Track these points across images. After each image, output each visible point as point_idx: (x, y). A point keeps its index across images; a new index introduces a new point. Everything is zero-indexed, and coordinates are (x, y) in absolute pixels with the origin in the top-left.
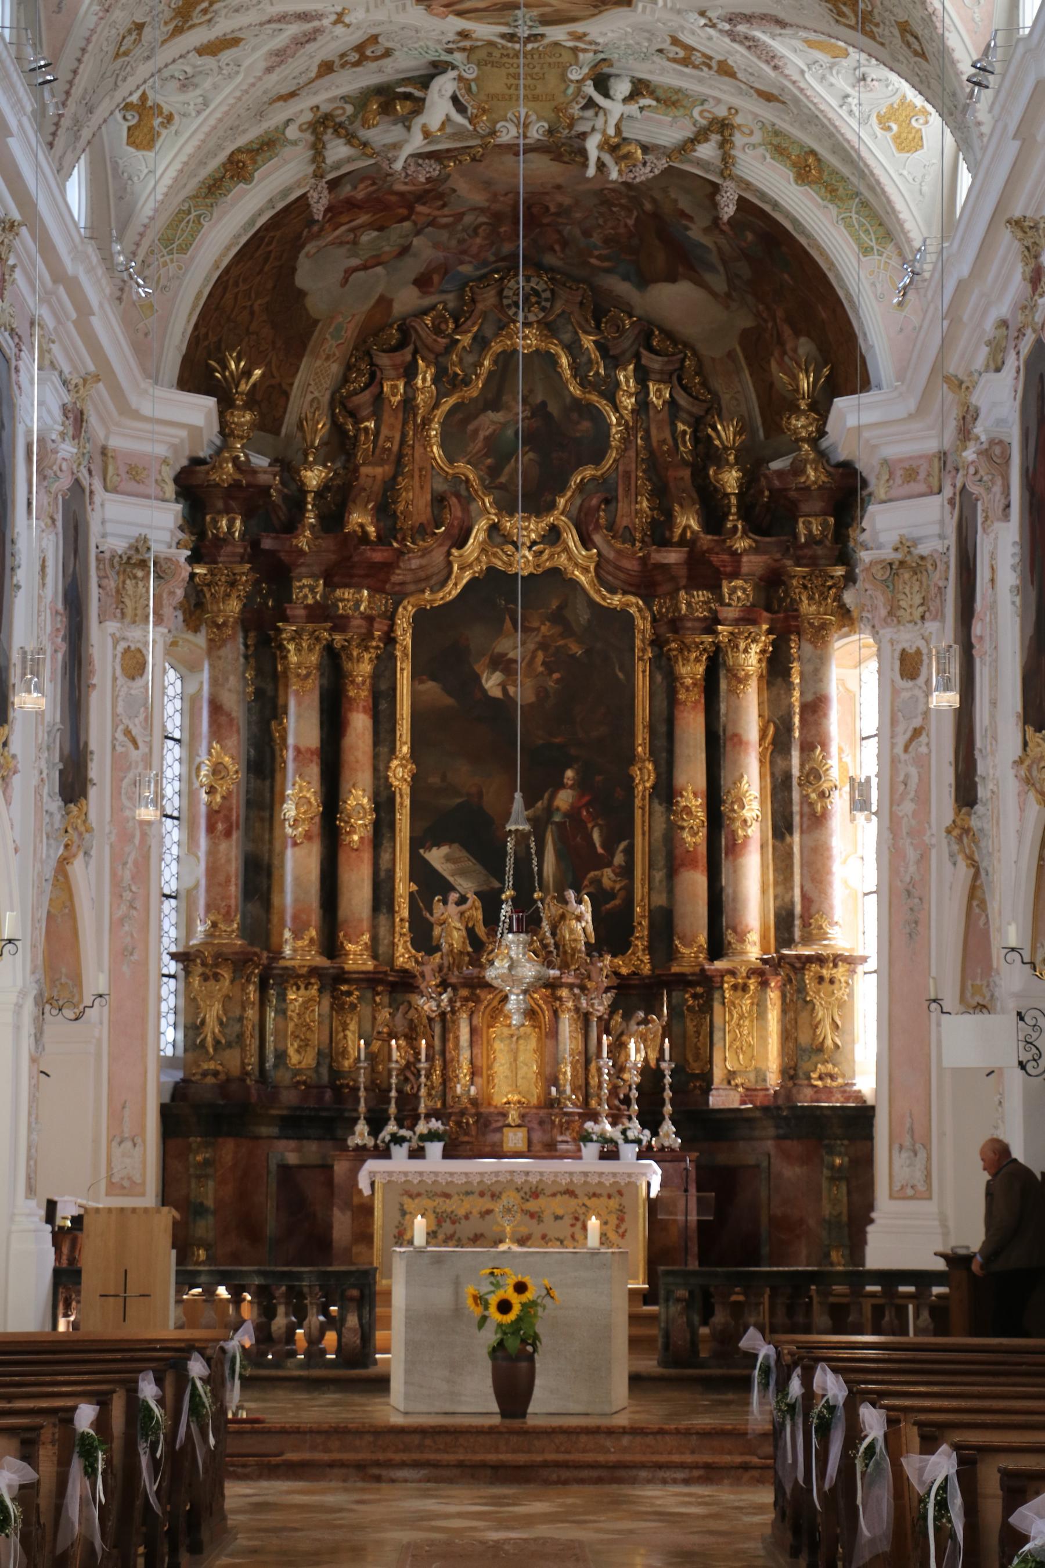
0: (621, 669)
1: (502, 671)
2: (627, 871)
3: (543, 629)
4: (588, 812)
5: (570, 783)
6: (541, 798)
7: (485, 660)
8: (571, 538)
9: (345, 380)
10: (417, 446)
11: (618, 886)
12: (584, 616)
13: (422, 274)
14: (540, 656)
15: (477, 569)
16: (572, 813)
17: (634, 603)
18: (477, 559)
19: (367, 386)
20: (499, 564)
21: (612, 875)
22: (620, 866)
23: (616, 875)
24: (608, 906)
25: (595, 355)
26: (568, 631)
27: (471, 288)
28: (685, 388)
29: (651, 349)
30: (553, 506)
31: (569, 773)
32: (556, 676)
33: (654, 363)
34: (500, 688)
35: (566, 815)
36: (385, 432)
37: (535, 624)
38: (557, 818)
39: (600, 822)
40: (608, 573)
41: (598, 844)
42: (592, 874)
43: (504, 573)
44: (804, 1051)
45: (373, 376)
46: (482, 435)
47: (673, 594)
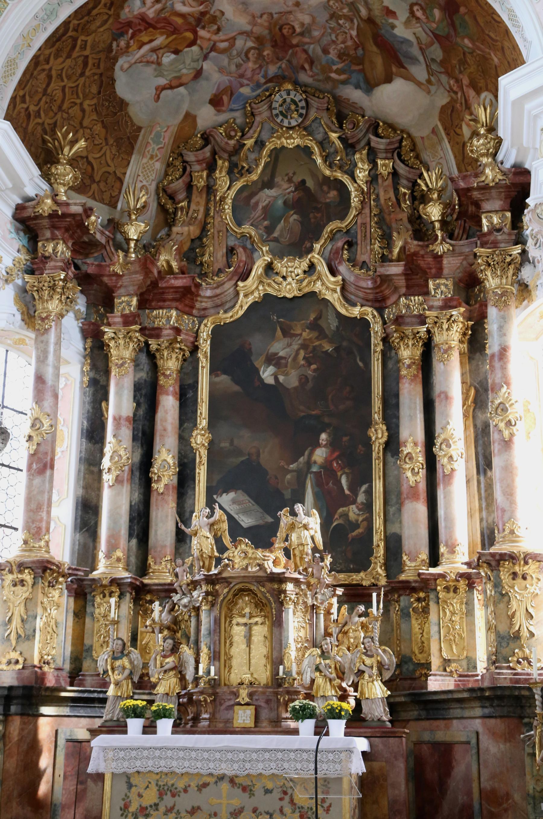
0: (360, 360)
1: (274, 365)
2: (368, 507)
3: (304, 334)
4: (337, 463)
5: (324, 443)
6: (303, 455)
7: (263, 358)
8: (322, 268)
9: (166, 174)
10: (216, 217)
11: (361, 519)
12: (333, 323)
13: (215, 95)
14: (302, 353)
15: (256, 294)
16: (327, 466)
17: (369, 313)
18: (257, 288)
19: (181, 177)
20: (270, 291)
21: (356, 510)
22: (362, 503)
23: (360, 510)
24: (354, 533)
25: (338, 143)
26: (322, 334)
27: (250, 105)
28: (403, 161)
29: (377, 135)
30: (310, 250)
31: (323, 436)
32: (313, 367)
33: (379, 144)
34: (273, 377)
35: (321, 467)
36: (193, 207)
37: (298, 332)
38: (315, 469)
39: (347, 470)
40: (351, 293)
41: (345, 487)
42: (341, 510)
43: (276, 297)
44: (503, 638)
45: (185, 169)
46: (260, 207)
47: (397, 302)
